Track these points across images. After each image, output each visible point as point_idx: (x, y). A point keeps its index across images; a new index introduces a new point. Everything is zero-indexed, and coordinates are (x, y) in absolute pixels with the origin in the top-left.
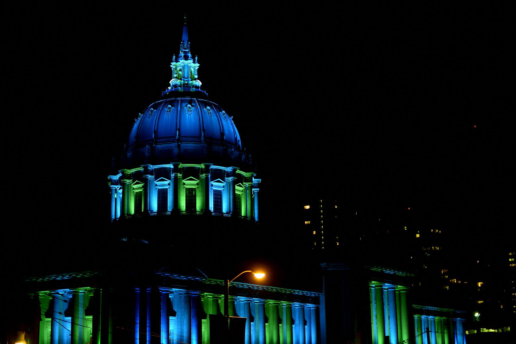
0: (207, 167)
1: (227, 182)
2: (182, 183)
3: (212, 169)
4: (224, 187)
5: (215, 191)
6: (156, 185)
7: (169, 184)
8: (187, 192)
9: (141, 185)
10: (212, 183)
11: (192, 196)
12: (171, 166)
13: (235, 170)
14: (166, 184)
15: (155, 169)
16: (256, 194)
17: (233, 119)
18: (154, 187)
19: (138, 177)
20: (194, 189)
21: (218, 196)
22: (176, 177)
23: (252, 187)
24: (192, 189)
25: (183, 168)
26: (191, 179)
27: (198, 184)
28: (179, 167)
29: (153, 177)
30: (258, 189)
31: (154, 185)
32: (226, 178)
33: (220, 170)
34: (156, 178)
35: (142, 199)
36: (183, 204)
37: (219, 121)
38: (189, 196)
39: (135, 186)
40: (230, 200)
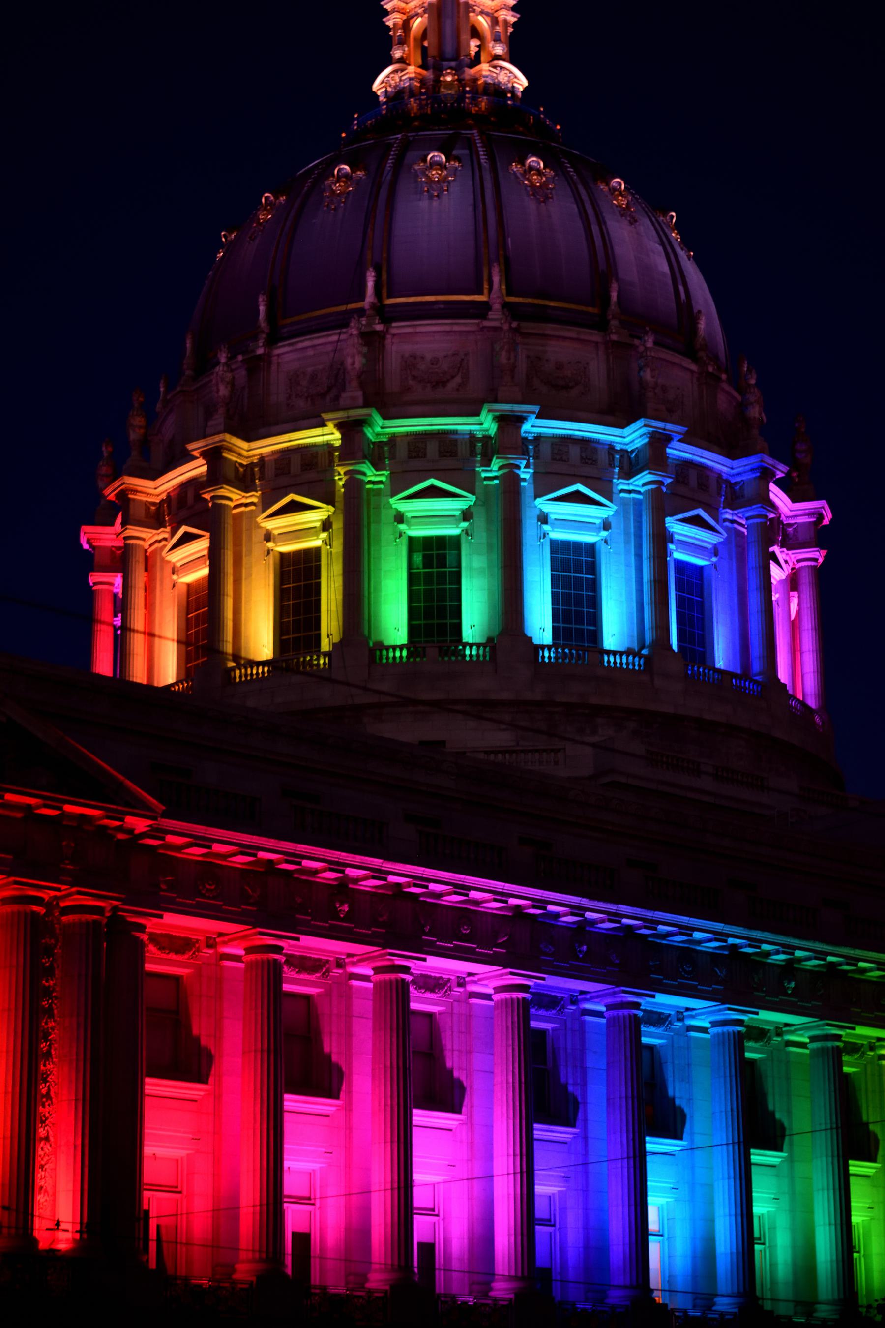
0: (509, 423)
1: (624, 503)
2: (387, 516)
3: (538, 438)
4: (606, 526)
5: (557, 547)
6: (268, 537)
7: (326, 525)
8: (418, 559)
9: (201, 546)
10: (544, 504)
11: (441, 576)
12: (329, 435)
13: (658, 441)
14: (307, 527)
15: (262, 458)
16: (806, 580)
17: (678, 227)
18: (258, 548)
19: (192, 511)
20: (454, 543)
21: (577, 572)
22: (354, 484)
23: (774, 532)
24: (441, 542)
25: (393, 439)
26: (433, 492)
27: (466, 515)
28: (369, 433)
29: (254, 497)
30: (818, 555)
31: (258, 536)
32: (620, 484)
33: (585, 443)
34: (266, 503)
35: (206, 614)
36: (393, 621)
37: (591, 218)
38: (428, 577)
39: (178, 557)
40: (640, 591)
